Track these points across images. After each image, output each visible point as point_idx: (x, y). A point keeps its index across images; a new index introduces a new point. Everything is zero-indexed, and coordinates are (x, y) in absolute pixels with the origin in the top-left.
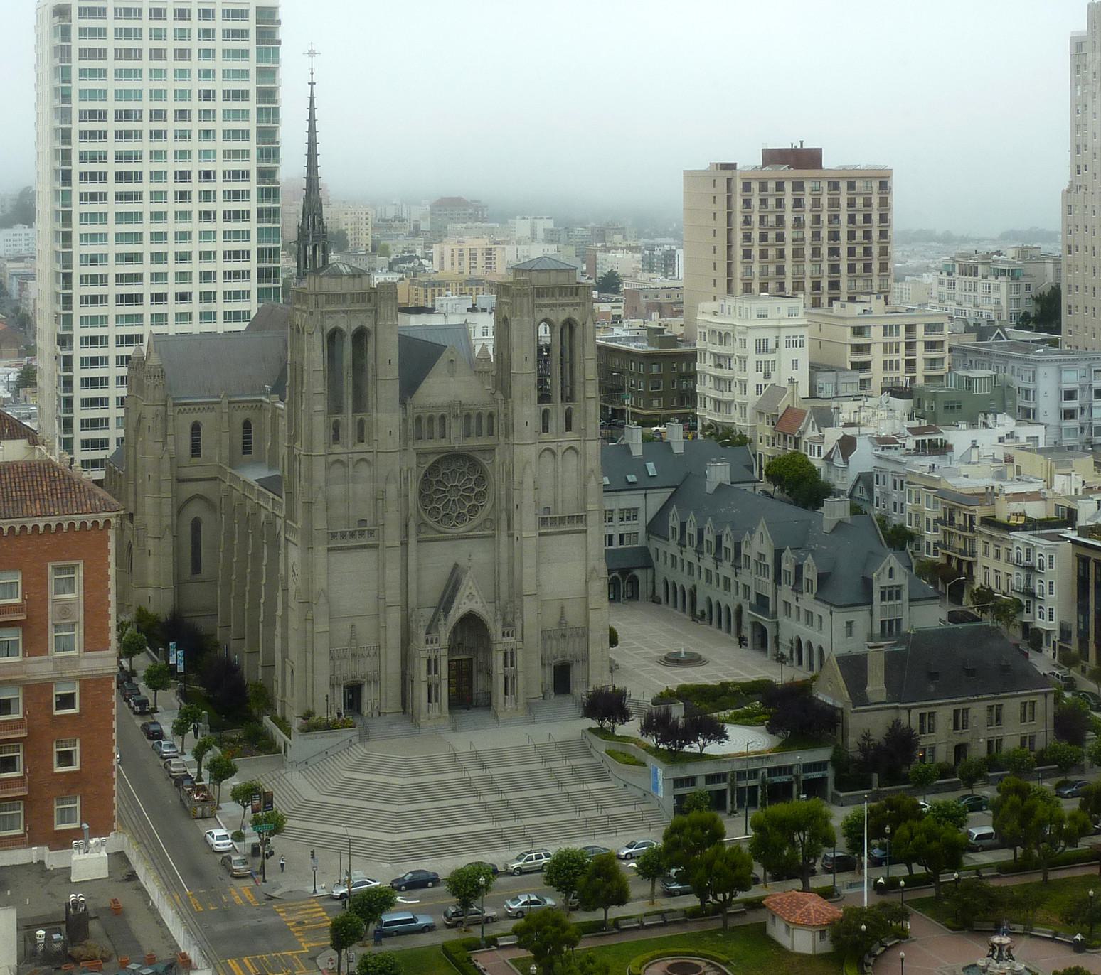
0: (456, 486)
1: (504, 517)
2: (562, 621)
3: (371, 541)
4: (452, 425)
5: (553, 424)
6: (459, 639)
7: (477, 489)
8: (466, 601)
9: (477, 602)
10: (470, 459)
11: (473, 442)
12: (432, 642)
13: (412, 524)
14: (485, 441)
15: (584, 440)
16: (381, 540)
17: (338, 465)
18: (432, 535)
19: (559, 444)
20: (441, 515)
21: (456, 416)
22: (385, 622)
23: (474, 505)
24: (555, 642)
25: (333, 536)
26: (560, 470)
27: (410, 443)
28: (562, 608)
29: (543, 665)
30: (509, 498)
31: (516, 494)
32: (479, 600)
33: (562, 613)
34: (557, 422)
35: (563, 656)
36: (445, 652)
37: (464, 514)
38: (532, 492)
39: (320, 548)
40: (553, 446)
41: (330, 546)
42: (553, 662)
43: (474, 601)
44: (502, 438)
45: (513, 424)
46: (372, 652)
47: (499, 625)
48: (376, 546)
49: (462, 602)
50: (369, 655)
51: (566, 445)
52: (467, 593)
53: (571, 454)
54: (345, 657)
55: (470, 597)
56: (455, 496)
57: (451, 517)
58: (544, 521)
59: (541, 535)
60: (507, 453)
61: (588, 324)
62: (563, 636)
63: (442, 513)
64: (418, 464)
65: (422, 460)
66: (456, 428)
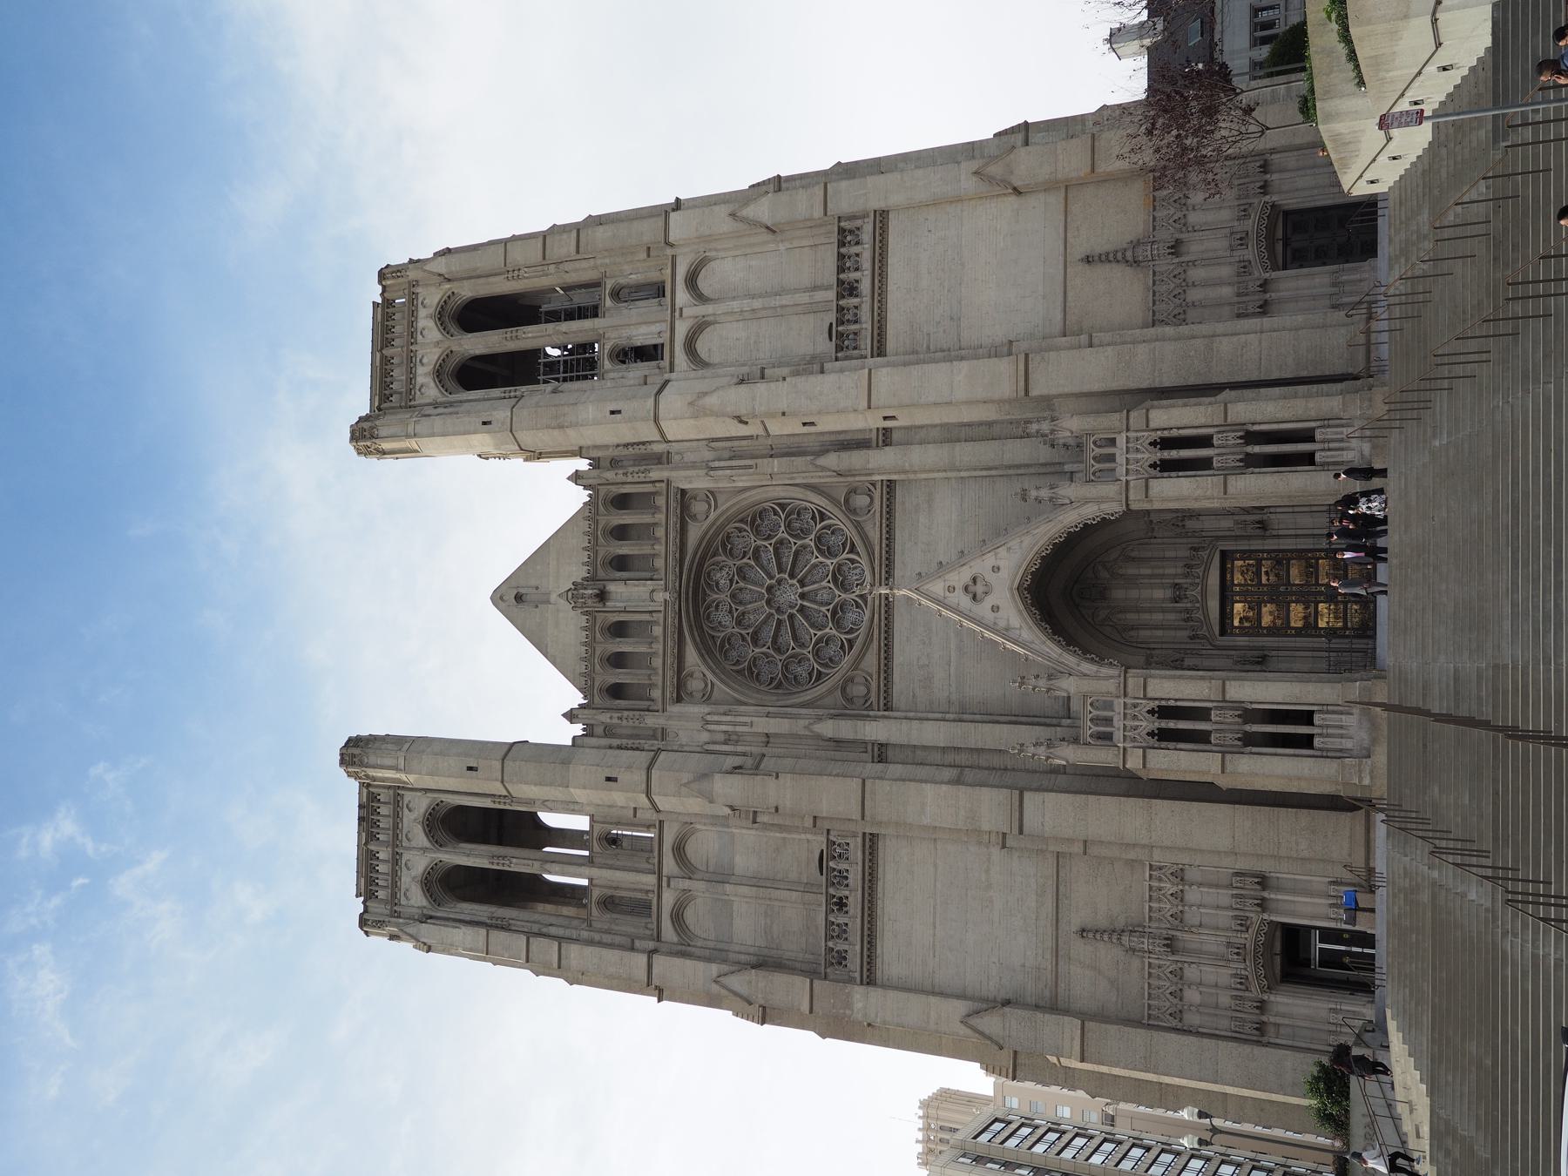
0: (770, 589)
1: (832, 460)
2: (1127, 256)
3: (856, 852)
4: (621, 605)
5: (643, 335)
6: (1159, 594)
7: (782, 533)
8: (989, 602)
9: (996, 569)
10: (707, 552)
11: (660, 551)
12: (1108, 721)
13: (828, 728)
14: (660, 518)
15: (668, 244)
16: (852, 827)
17: (689, 916)
18: (871, 662)
19: (677, 314)
20: (834, 632)
21: (602, 596)
22: (1070, 841)
23: (819, 539)
24: (1196, 274)
25: (841, 958)
26: (735, 305)
27: (651, 721)
28: (1088, 260)
29: (1264, 309)
30: (790, 450)
31: (777, 428)
32: (990, 560)
33: (1106, 258)
34: (638, 323)
35: (1243, 241)
36: (1134, 682)
37: (839, 566)
38: (761, 387)
39: (858, 1005)
40: (682, 329)
41: (857, 975)
42: (1259, 273)
43: (991, 577)
44: (655, 474)
45: (626, 445)
46: (1169, 887)
47: (1068, 491)
48: (871, 843)
49: (989, 616)
50: (1179, 897)
51: (682, 296)
52: (965, 601)
53: (704, 284)
54: (1178, 974)
55: (979, 589)
56: (789, 594)
57: (842, 606)
58: (843, 341)
59: (880, 350)
60: (689, 457)
61: (443, 270)
62: (1176, 248)
63: (830, 631)
64: (707, 698)
65: (695, 685)
66: (628, 594)
